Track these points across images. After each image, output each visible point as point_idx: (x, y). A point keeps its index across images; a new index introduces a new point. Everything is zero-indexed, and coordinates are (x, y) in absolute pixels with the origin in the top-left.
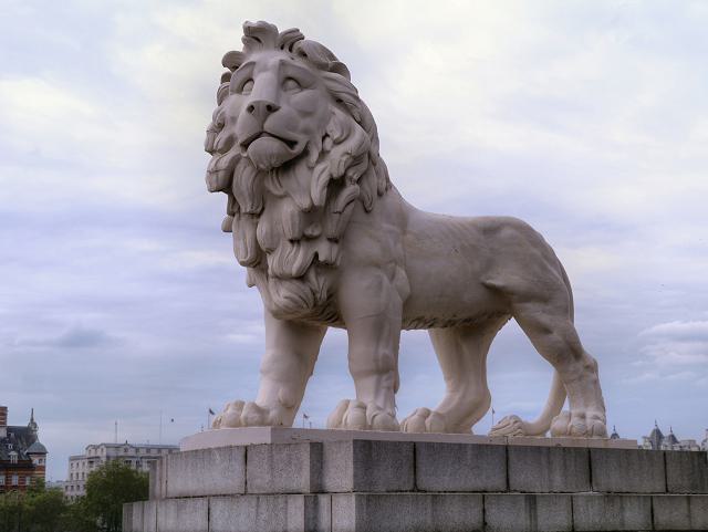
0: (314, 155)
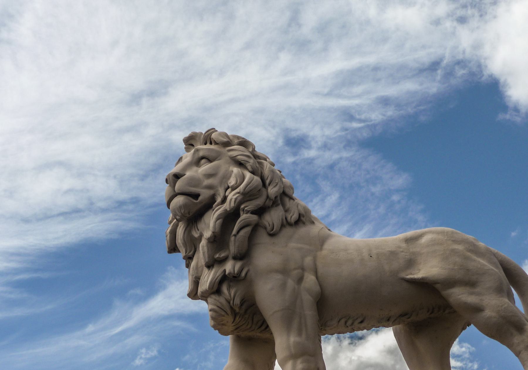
0: (219, 200)
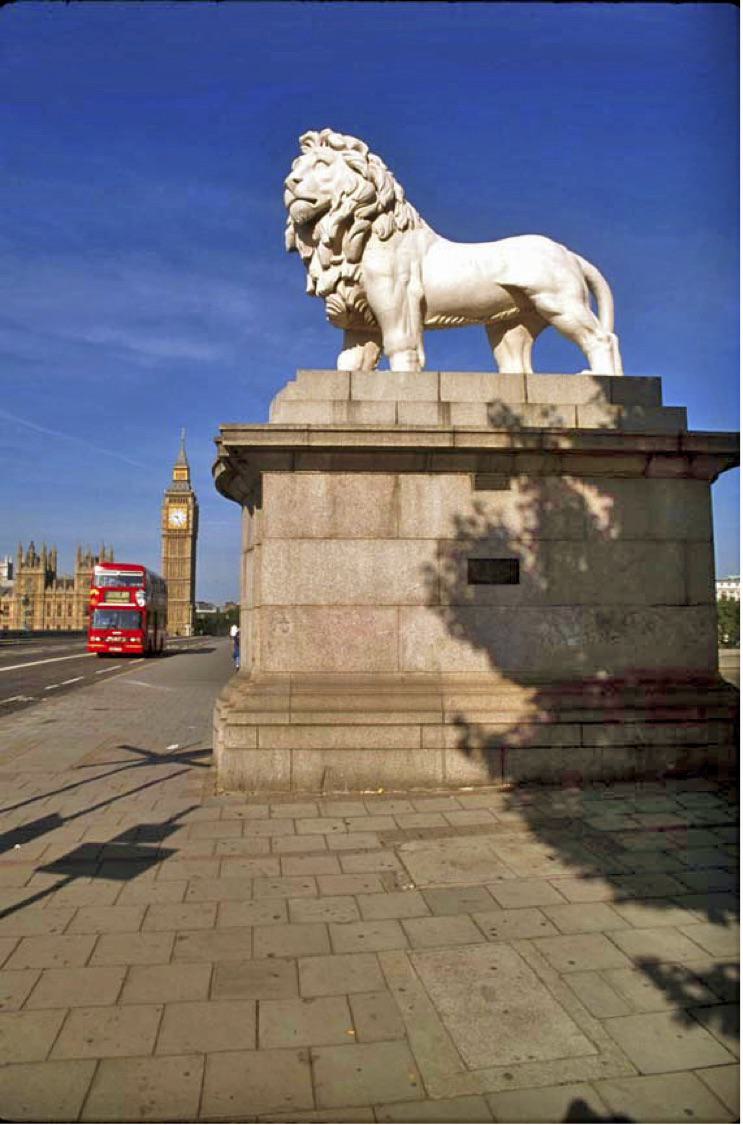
0: (334, 205)
